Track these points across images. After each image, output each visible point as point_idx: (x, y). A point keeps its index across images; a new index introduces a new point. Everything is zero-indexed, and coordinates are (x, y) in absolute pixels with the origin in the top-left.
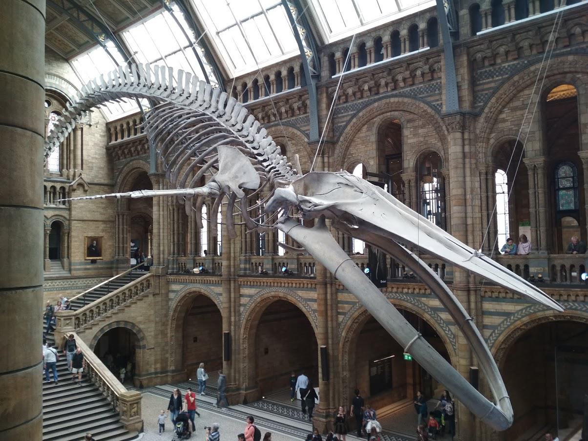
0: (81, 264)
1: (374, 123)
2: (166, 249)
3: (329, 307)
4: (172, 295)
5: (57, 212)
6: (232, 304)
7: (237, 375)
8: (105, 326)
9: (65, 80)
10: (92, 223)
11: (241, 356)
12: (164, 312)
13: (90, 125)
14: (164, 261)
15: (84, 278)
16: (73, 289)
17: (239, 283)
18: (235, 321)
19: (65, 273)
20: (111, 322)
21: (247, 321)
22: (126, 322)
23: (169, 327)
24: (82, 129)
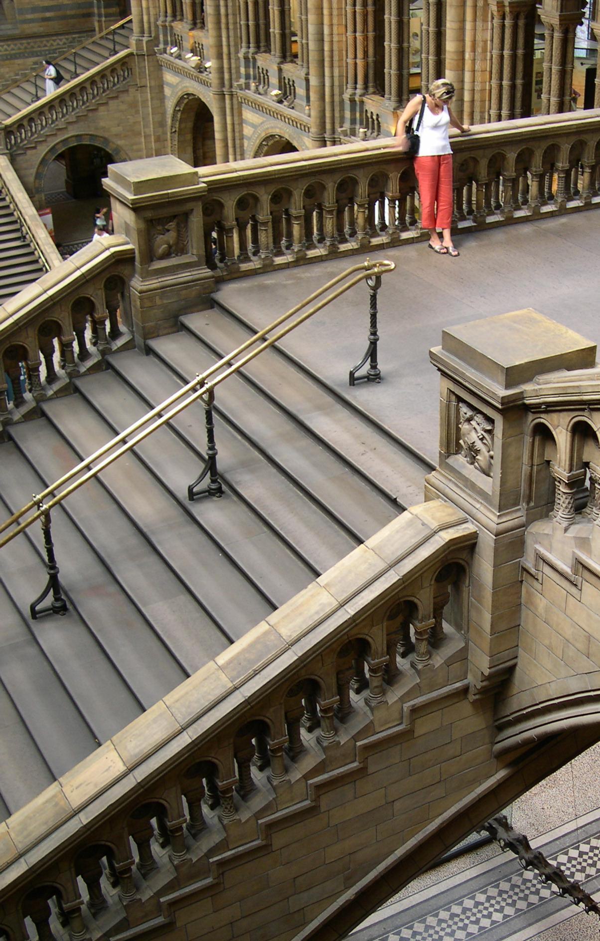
4: (167, 91)
6: (230, 135)
8: (57, 144)
14: (150, 28)
15: (43, 36)
16: (27, 57)
17: (240, 100)
20: (66, 136)
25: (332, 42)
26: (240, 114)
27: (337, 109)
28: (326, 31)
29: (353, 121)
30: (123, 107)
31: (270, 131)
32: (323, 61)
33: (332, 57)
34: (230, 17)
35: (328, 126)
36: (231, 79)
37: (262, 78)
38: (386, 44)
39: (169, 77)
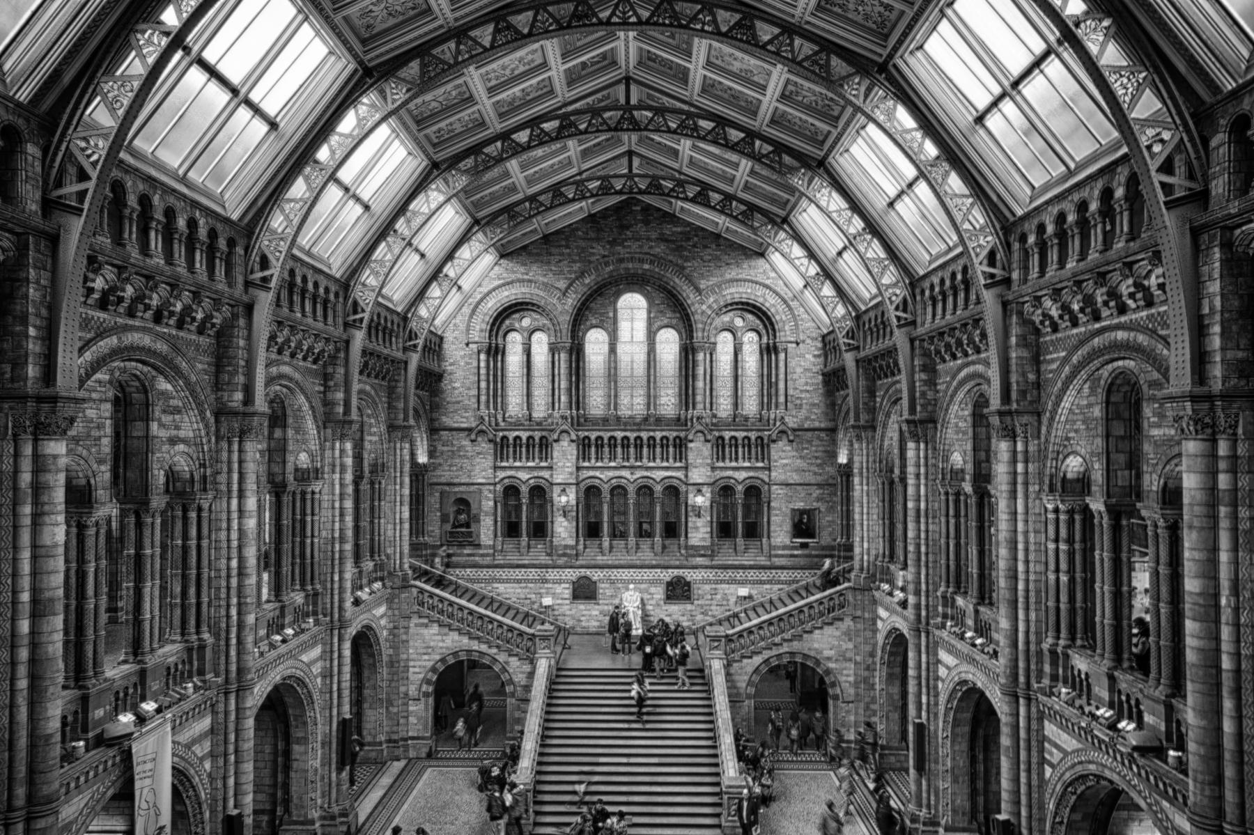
0: (784, 548)
1: (1099, 379)
2: (873, 546)
3: (1022, 743)
4: (880, 624)
5: (751, 474)
6: (924, 674)
7: (932, 798)
9: (760, 284)
10: (799, 488)
11: (940, 767)
12: (868, 648)
13: (798, 344)
18: (928, 704)
19: (762, 560)
21: (947, 710)
22: (806, 656)
23: (877, 674)
24: (786, 350)
25: (1027, 581)
26: (936, 654)
27: (1033, 661)
28: (1021, 567)
29: (1055, 678)
30: (838, 633)
31: (963, 675)
32: (1016, 601)
33: (1027, 598)
34: (930, 556)
35: (1022, 679)
36: (927, 617)
37: (959, 619)
38: (1097, 585)
39: (882, 613)
